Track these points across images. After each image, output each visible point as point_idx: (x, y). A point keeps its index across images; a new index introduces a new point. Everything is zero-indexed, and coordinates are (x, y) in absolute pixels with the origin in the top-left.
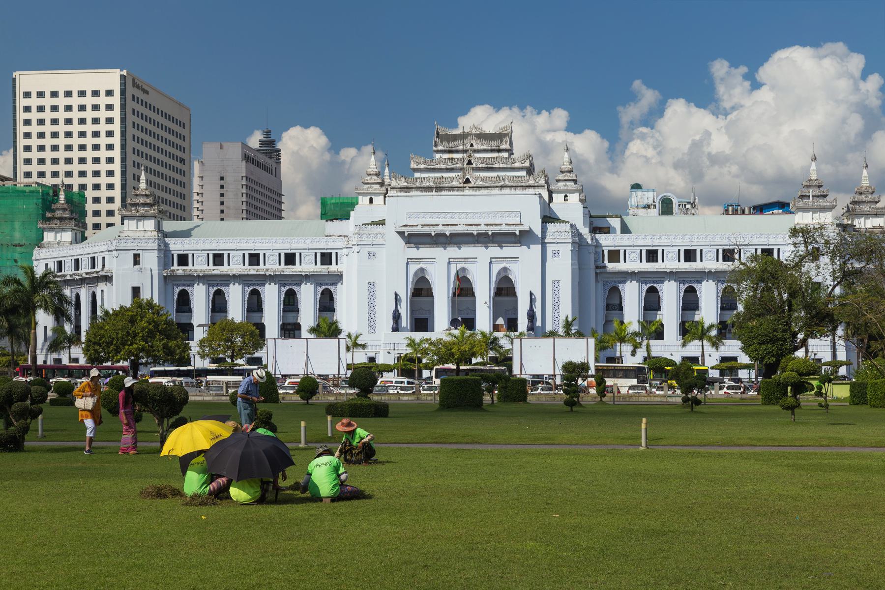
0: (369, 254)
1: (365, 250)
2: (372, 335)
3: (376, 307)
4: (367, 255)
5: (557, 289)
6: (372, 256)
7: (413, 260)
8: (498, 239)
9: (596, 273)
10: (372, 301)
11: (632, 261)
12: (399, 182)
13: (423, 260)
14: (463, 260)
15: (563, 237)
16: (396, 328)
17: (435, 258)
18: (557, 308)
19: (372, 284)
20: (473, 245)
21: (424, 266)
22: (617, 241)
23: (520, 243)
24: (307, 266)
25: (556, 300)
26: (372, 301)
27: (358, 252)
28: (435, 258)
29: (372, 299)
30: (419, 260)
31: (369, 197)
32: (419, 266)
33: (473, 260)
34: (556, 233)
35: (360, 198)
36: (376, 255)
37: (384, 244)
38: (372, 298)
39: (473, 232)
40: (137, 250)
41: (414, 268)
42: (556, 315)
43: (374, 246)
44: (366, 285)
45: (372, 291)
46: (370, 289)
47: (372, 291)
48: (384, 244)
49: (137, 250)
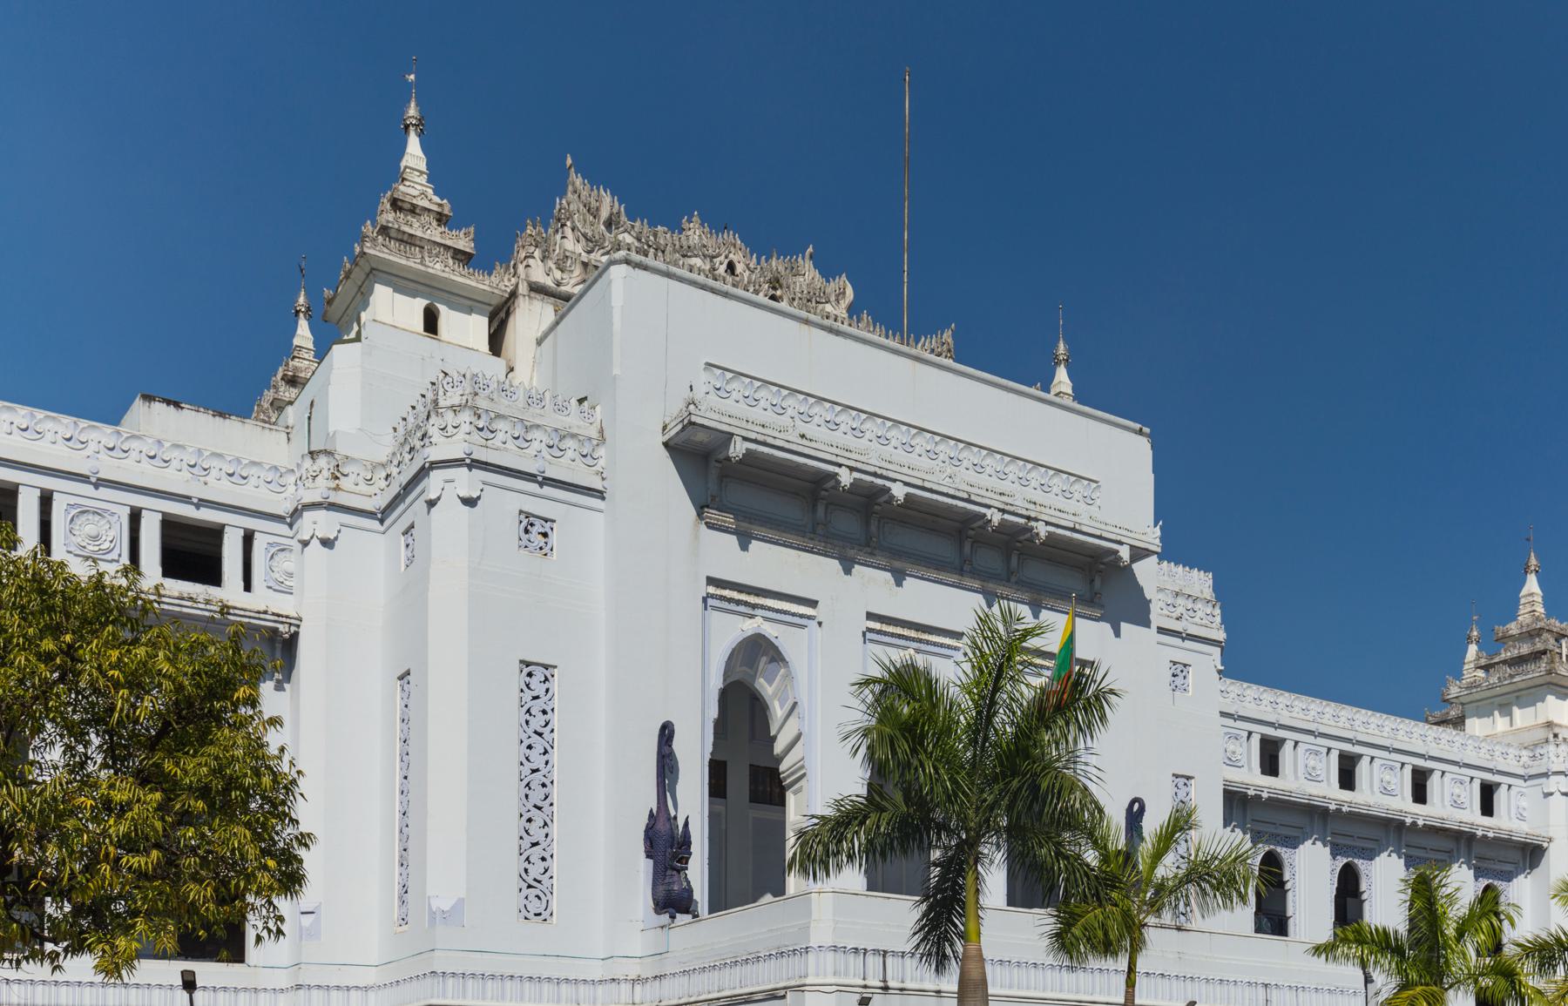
0: (528, 521)
1: (506, 501)
2: (535, 925)
3: (555, 792)
4: (513, 528)
7: (727, 593)
8: (1035, 571)
10: (538, 761)
12: (558, 275)
14: (913, 634)
15: (1197, 620)
16: (673, 902)
17: (813, 603)
19: (539, 674)
20: (954, 579)
21: (770, 630)
23: (1102, 607)
26: (538, 761)
27: (470, 502)
28: (813, 603)
30: (752, 599)
31: (428, 302)
32: (749, 627)
33: (947, 641)
34: (1180, 601)
35: (382, 294)
36: (554, 538)
37: (600, 494)
38: (539, 744)
39: (988, 512)
41: (732, 629)
43: (547, 490)
44: (518, 680)
45: (536, 707)
46: (528, 695)
47: (536, 707)
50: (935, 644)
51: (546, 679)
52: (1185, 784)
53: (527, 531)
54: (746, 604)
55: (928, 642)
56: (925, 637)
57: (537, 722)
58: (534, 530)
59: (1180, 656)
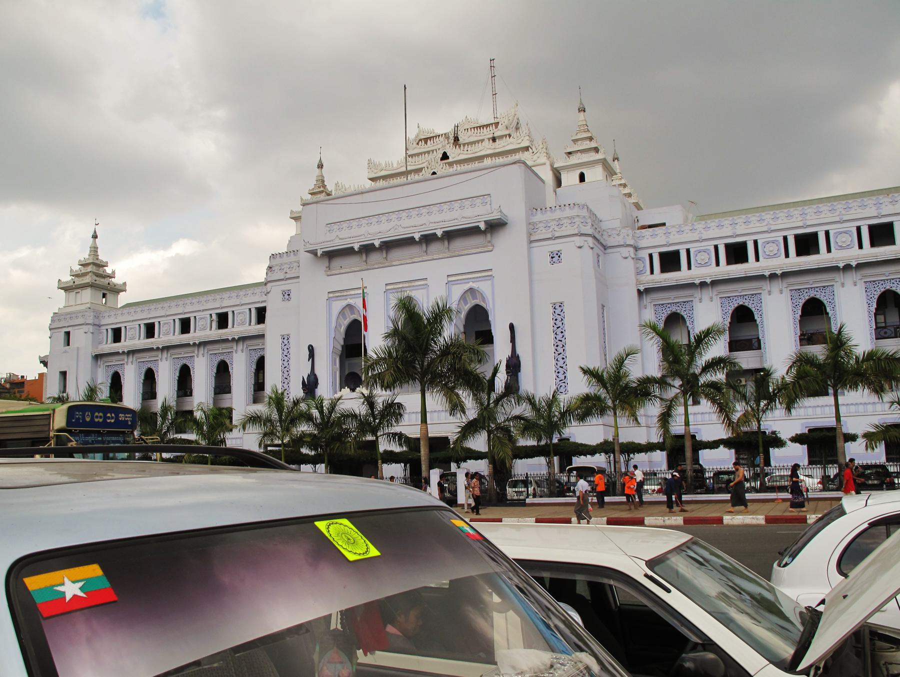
5: (559, 318)
6: (286, 296)
9: (639, 291)
11: (701, 265)
13: (352, 292)
14: (407, 285)
18: (560, 350)
22: (671, 236)
24: (240, 326)
25: (559, 337)
29: (286, 360)
32: (345, 303)
40: (68, 327)
42: (561, 363)
48: (298, 277)
49: (68, 327)
50: (417, 286)
51: (288, 339)
52: (560, 306)
53: (284, 296)
54: (343, 296)
55: (413, 286)
56: (413, 284)
57: (285, 353)
58: (286, 295)
59: (555, 248)
